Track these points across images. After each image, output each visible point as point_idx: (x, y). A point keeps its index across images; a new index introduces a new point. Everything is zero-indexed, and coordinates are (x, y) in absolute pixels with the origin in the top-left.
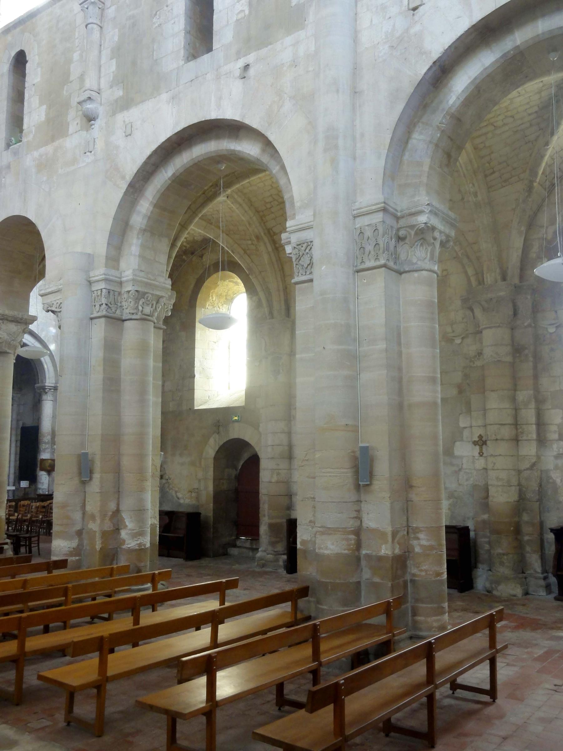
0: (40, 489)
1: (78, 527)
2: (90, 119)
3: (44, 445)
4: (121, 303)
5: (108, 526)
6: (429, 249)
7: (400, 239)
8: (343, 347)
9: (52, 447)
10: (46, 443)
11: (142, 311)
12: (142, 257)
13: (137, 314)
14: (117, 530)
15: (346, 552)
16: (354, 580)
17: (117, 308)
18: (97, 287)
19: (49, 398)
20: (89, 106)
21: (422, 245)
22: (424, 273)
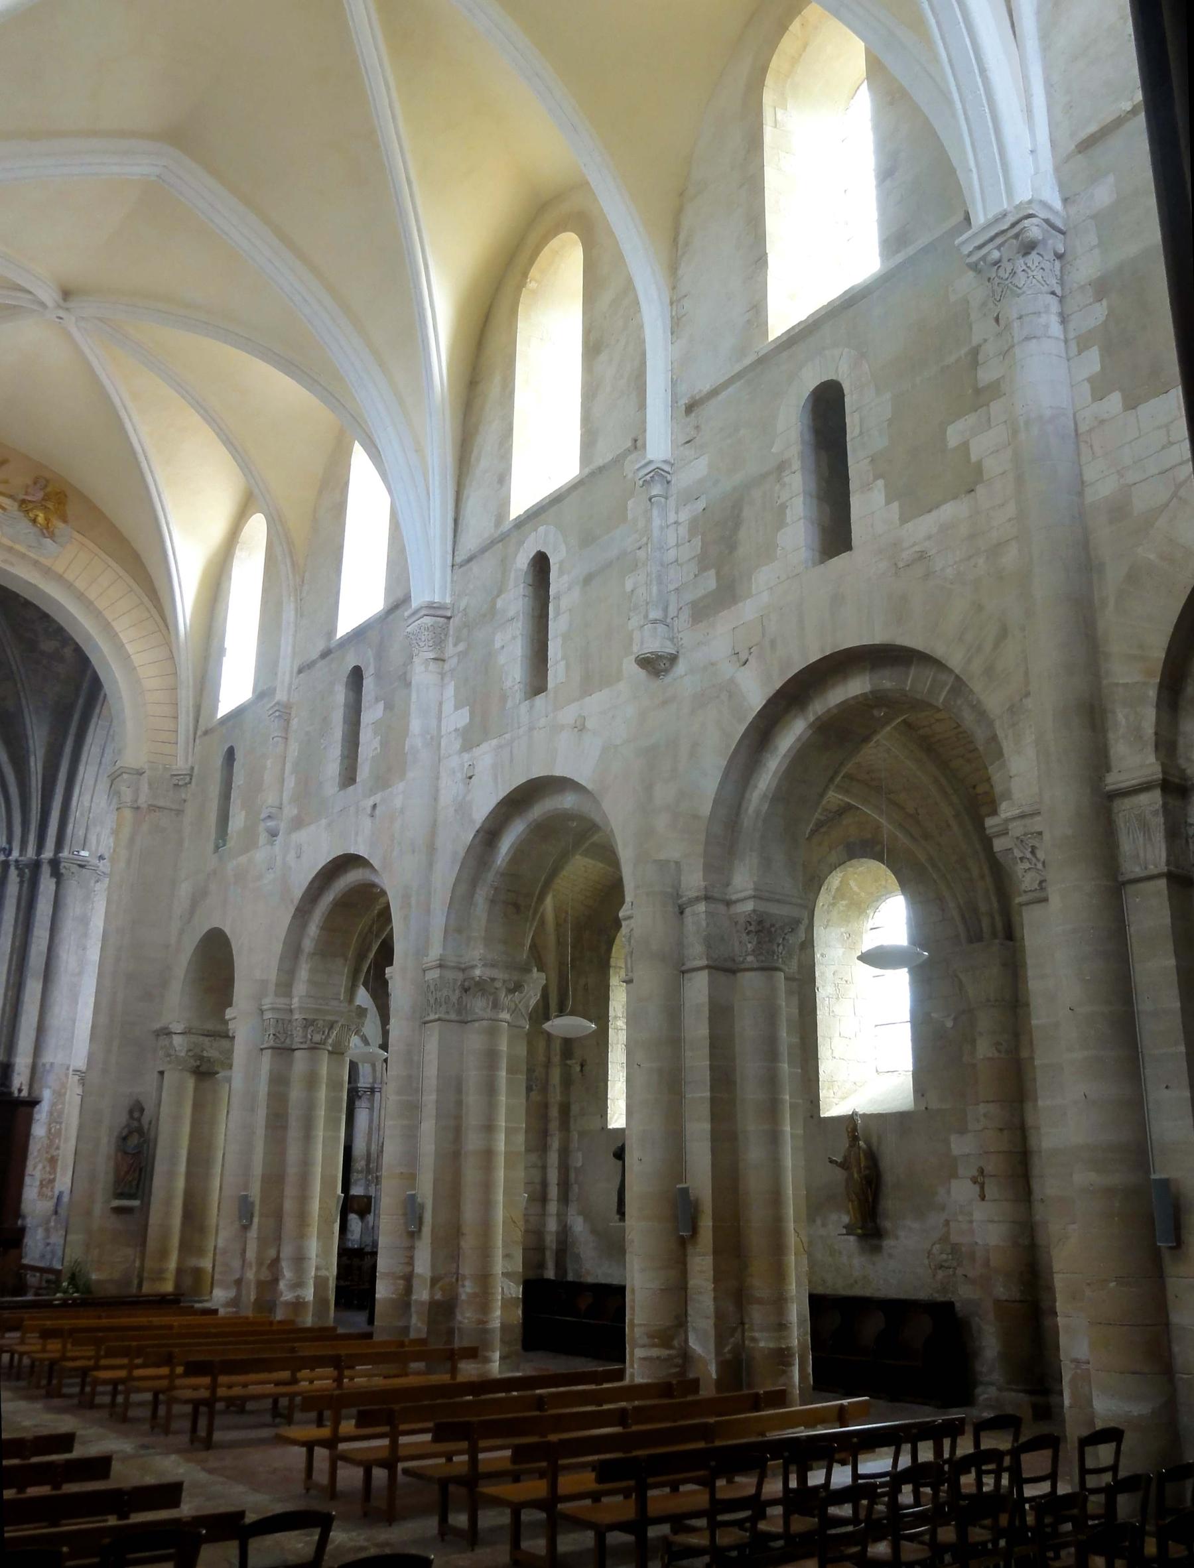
0: (349, 1240)
1: (237, 1276)
2: (273, 834)
3: (355, 1174)
4: (291, 1031)
5: (265, 1275)
6: (491, 998)
7: (466, 990)
8: (404, 1098)
9: (366, 1178)
10: (358, 1172)
11: (311, 1040)
12: (311, 982)
13: (306, 1043)
14: (275, 1280)
15: (394, 1296)
16: (401, 1324)
17: (286, 1037)
18: (268, 1015)
19: (364, 1105)
20: (271, 824)
21: (483, 995)
22: (485, 1023)
